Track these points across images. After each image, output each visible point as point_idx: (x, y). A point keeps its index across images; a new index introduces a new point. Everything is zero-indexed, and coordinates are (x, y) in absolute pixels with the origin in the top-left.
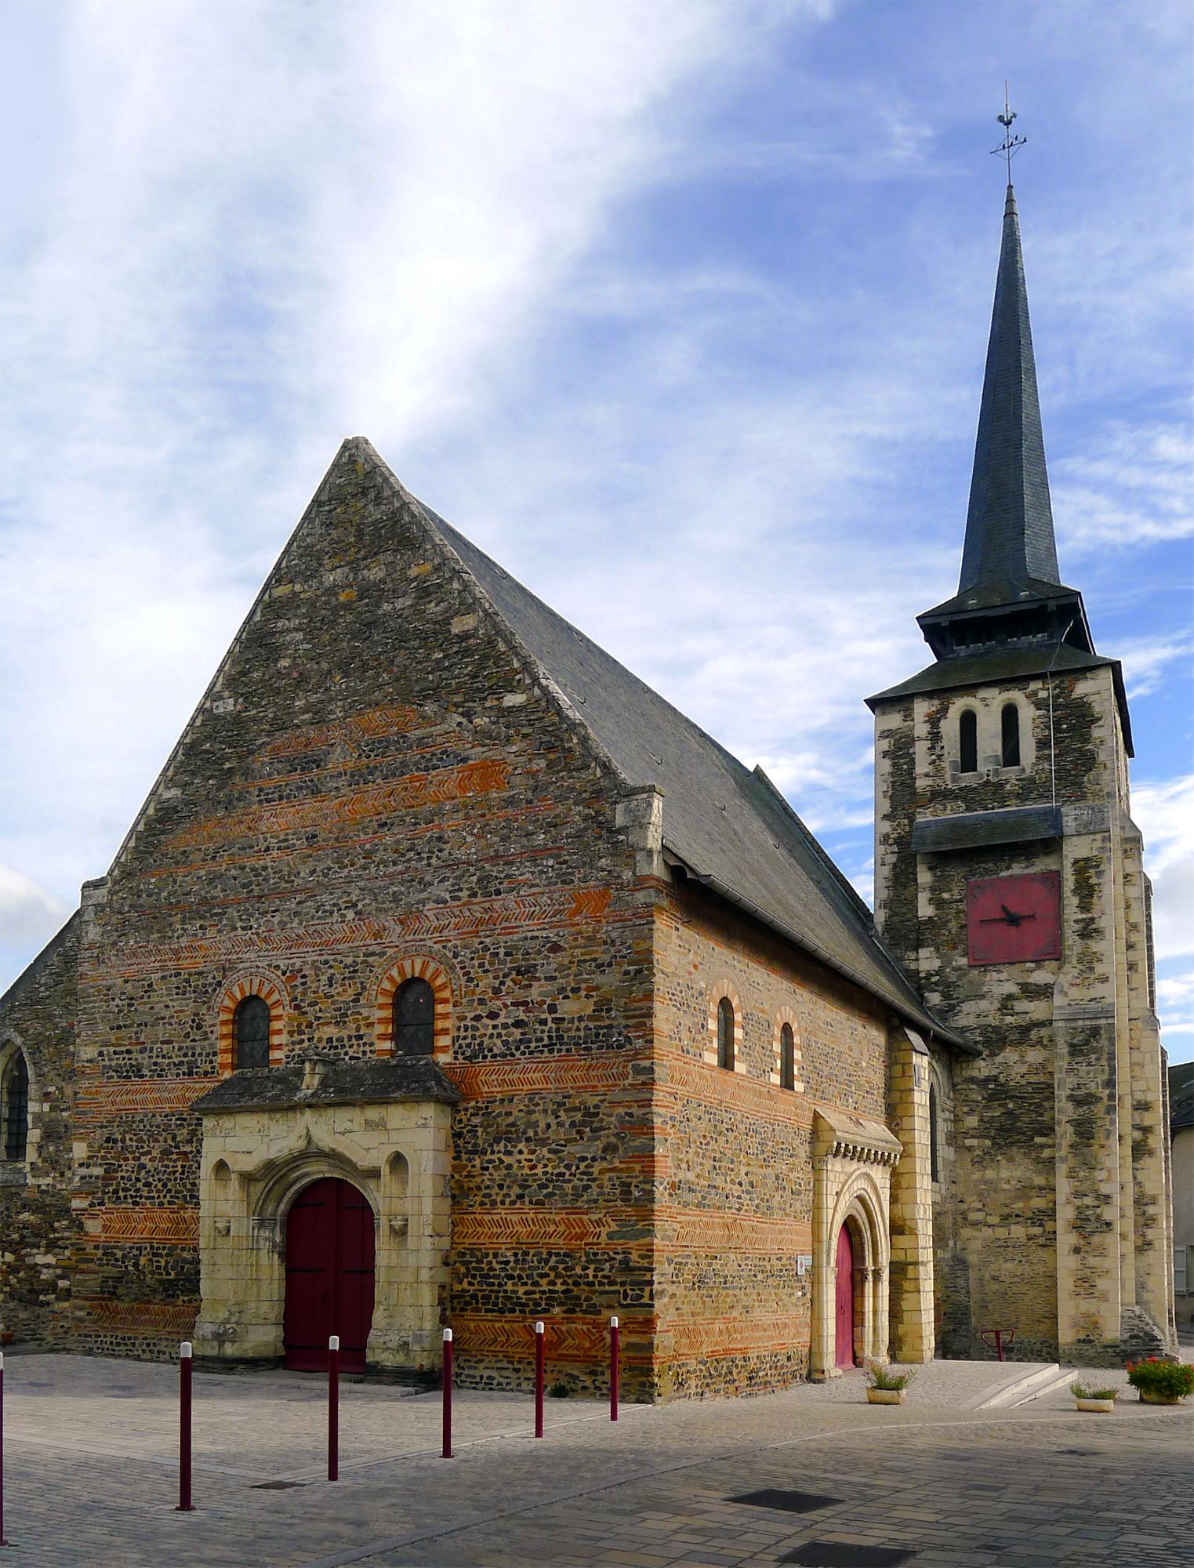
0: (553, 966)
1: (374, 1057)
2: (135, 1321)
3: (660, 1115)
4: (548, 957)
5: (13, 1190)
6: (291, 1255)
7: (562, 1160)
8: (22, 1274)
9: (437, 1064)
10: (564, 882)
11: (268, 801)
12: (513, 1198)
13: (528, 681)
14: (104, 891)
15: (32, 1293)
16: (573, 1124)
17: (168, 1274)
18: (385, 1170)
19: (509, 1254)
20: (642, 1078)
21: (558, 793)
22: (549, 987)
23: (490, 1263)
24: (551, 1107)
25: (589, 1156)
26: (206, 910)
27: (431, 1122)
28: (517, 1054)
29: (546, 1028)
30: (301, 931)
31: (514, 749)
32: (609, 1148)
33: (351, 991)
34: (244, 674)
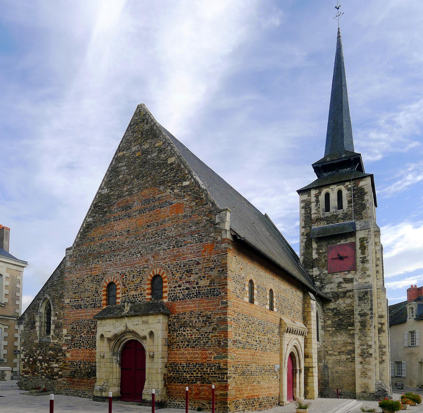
0: (197, 269)
1: (146, 300)
2: (79, 385)
3: (230, 318)
4: (195, 267)
5: (47, 344)
6: (123, 364)
7: (200, 333)
8: (49, 370)
9: (163, 302)
10: (201, 242)
11: (116, 220)
12: (186, 346)
13: (190, 177)
14: (71, 251)
15: (52, 376)
17: (88, 370)
18: (148, 337)
19: (184, 364)
20: (224, 305)
21: (199, 213)
22: (197, 276)
23: (179, 367)
24: (197, 316)
25: (208, 331)
26: (99, 256)
27: (161, 321)
28: (187, 298)
30: (125, 261)
31: (186, 199)
32: (214, 329)
33: (139, 280)
34: (110, 181)
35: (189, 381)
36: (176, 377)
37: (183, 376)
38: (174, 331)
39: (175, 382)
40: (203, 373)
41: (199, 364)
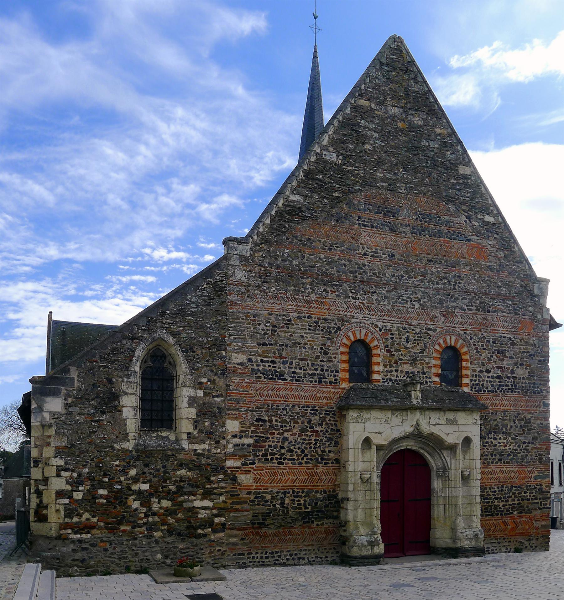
1: (432, 385)
16: (521, 426)
23: (488, 492)
24: (512, 418)
25: (527, 441)
29: (510, 381)
35: (503, 511)
37: (495, 505)
40: (520, 499)
41: (515, 487)
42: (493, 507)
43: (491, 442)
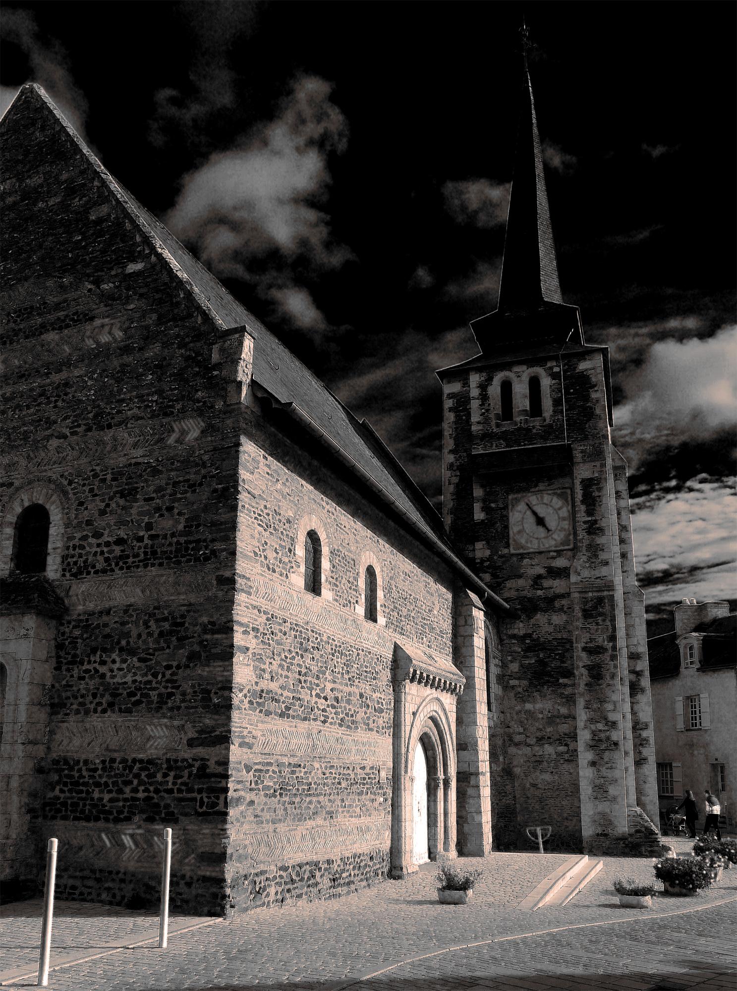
0: (152, 488)
4: (146, 481)
7: (149, 668)
13: (147, 252)
16: (161, 634)
19: (97, 761)
23: (80, 770)
25: (175, 664)
31: (132, 306)
36: (69, 802)
38: (73, 663)
39: (65, 818)
42: (88, 802)
43: (95, 668)
